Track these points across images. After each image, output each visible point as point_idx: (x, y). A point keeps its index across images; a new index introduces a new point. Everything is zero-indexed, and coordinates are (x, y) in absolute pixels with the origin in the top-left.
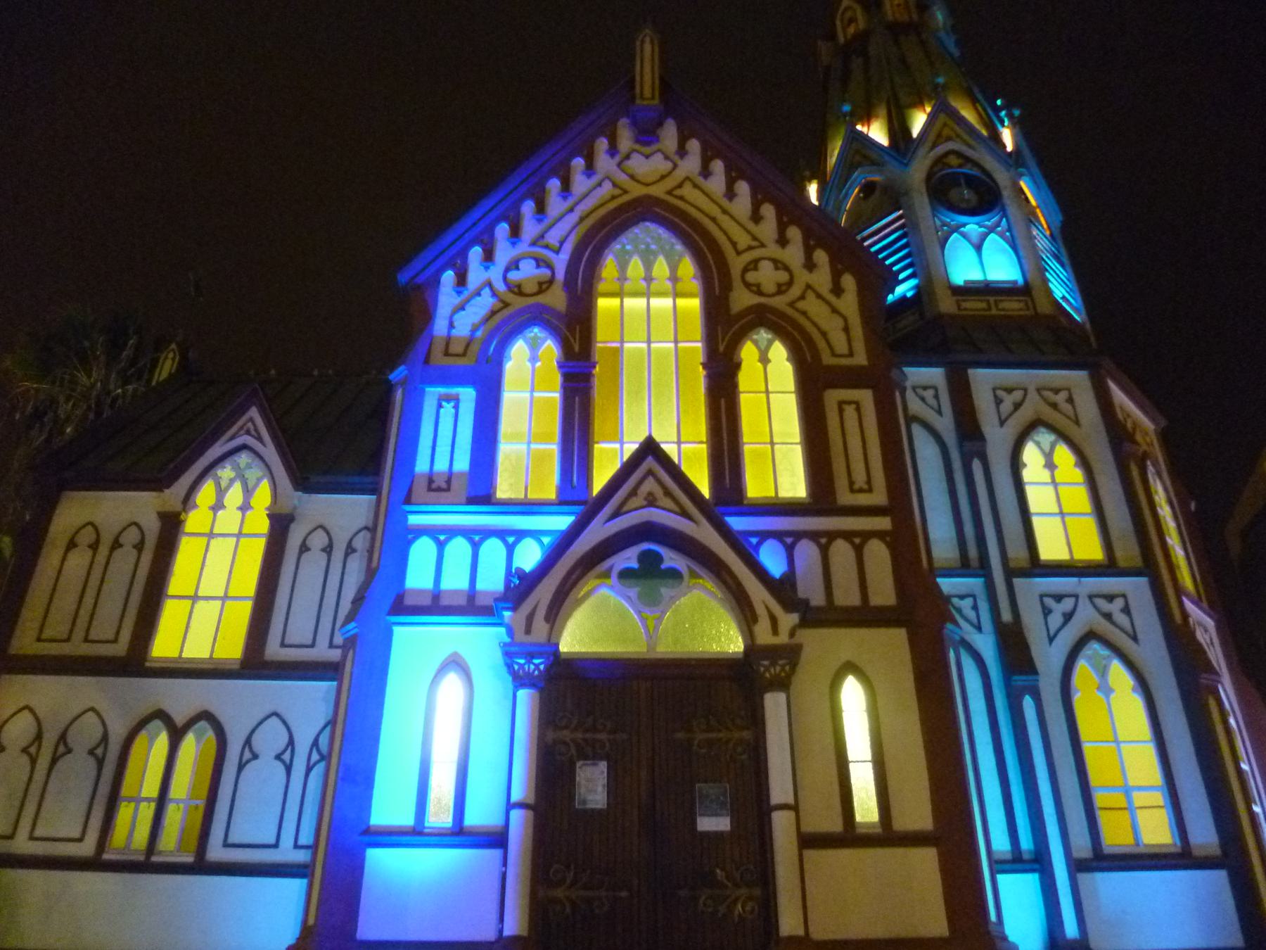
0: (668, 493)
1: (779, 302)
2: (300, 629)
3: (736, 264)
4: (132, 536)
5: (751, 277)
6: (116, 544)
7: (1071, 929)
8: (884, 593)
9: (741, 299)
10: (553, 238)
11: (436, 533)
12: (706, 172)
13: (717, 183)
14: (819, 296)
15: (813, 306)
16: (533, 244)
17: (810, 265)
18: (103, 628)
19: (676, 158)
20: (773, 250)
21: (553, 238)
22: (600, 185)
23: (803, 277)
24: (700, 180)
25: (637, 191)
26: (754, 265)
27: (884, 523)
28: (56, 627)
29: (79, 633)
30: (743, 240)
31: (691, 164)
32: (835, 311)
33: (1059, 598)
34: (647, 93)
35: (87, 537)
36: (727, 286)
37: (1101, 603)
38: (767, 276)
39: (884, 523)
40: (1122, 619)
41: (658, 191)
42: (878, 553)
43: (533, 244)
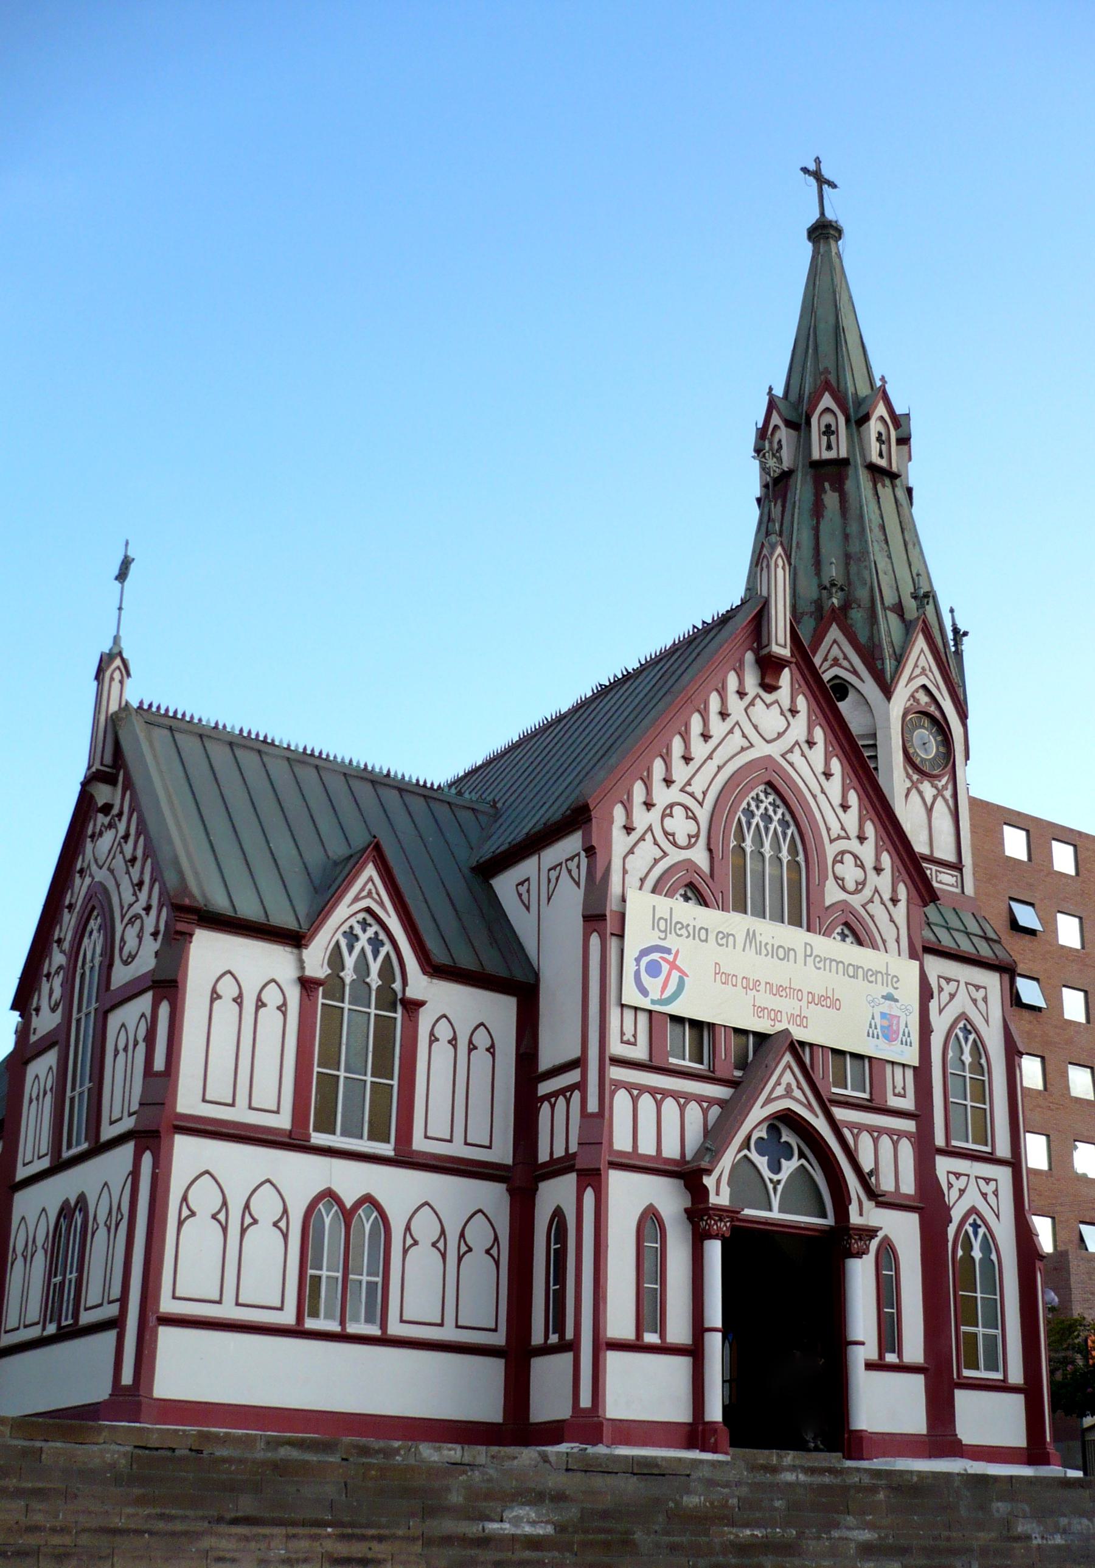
0: (800, 1087)
1: (856, 901)
3: (831, 851)
4: (272, 997)
6: (260, 1004)
8: (908, 1186)
9: (832, 894)
10: (697, 788)
11: (629, 1087)
14: (883, 903)
15: (876, 909)
16: (682, 790)
17: (878, 870)
18: (265, 1096)
19: (788, 714)
20: (854, 845)
21: (697, 788)
22: (731, 731)
24: (805, 747)
25: (761, 750)
26: (839, 859)
28: (219, 1090)
32: (892, 920)
33: (958, 1175)
34: (781, 641)
37: (981, 1182)
38: (849, 872)
40: (991, 1198)
41: (774, 750)
42: (906, 1149)
43: (682, 790)
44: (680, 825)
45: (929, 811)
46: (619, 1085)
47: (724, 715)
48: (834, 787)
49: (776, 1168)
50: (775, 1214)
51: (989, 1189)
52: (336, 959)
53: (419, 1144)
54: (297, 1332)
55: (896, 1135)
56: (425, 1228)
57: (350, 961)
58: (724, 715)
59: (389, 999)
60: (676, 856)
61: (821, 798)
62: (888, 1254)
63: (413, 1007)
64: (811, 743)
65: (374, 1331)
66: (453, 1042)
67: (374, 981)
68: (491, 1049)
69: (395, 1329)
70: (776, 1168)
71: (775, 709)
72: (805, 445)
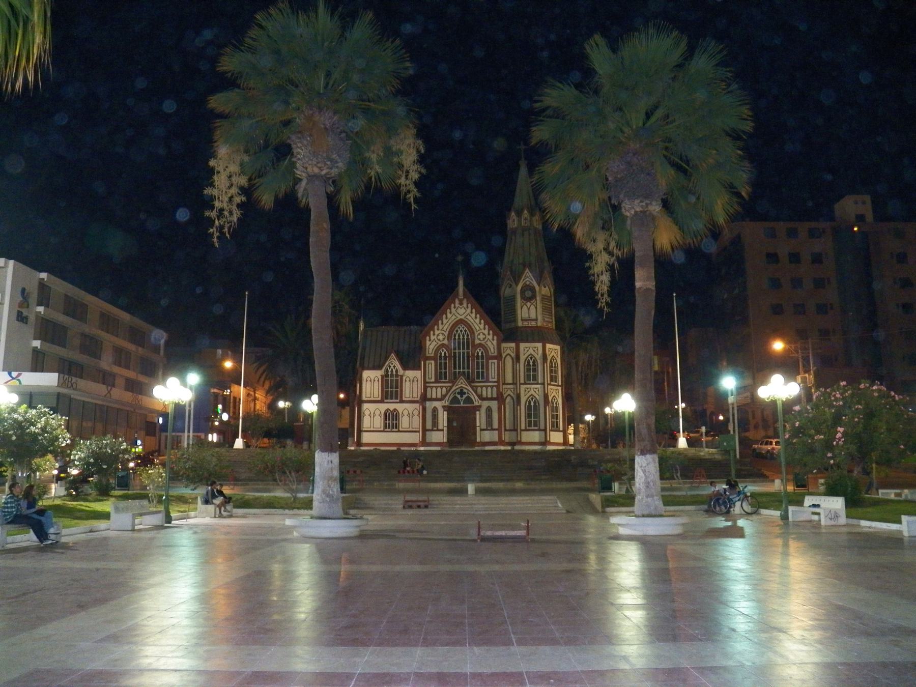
2: (408, 395)
4: (376, 379)
5: (479, 337)
7: (519, 439)
8: (495, 396)
9: (477, 342)
12: (472, 312)
13: (473, 315)
15: (489, 343)
17: (489, 334)
23: (488, 337)
25: (460, 317)
26: (479, 334)
27: (496, 384)
28: (368, 395)
29: (372, 396)
30: (478, 328)
31: (469, 311)
35: (369, 379)
36: (474, 339)
39: (496, 384)
41: (462, 317)
42: (495, 389)
44: (441, 337)
45: (529, 309)
46: (429, 387)
47: (451, 313)
48: (478, 320)
49: (462, 396)
50: (462, 405)
51: (537, 390)
52: (387, 371)
53: (404, 399)
54: (383, 431)
55: (492, 387)
56: (406, 413)
57: (390, 370)
58: (451, 313)
59: (397, 375)
60: (440, 343)
61: (475, 324)
62: (489, 410)
63: (402, 377)
64: (472, 312)
65: (397, 430)
66: (410, 381)
67: (394, 373)
68: (417, 381)
69: (401, 429)
70: (462, 396)
71: (463, 309)
72: (520, 221)
